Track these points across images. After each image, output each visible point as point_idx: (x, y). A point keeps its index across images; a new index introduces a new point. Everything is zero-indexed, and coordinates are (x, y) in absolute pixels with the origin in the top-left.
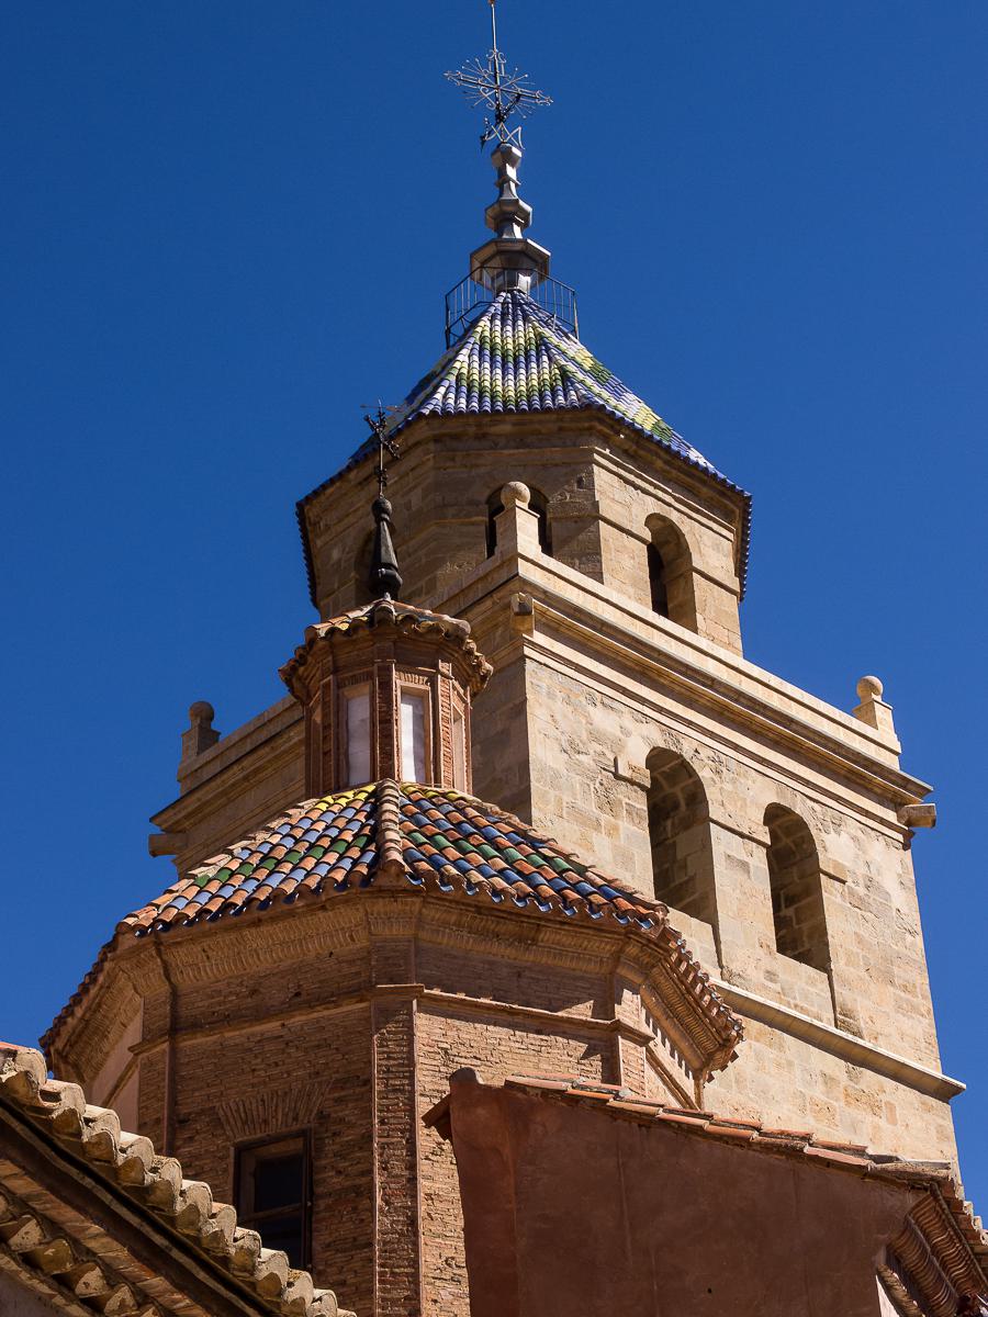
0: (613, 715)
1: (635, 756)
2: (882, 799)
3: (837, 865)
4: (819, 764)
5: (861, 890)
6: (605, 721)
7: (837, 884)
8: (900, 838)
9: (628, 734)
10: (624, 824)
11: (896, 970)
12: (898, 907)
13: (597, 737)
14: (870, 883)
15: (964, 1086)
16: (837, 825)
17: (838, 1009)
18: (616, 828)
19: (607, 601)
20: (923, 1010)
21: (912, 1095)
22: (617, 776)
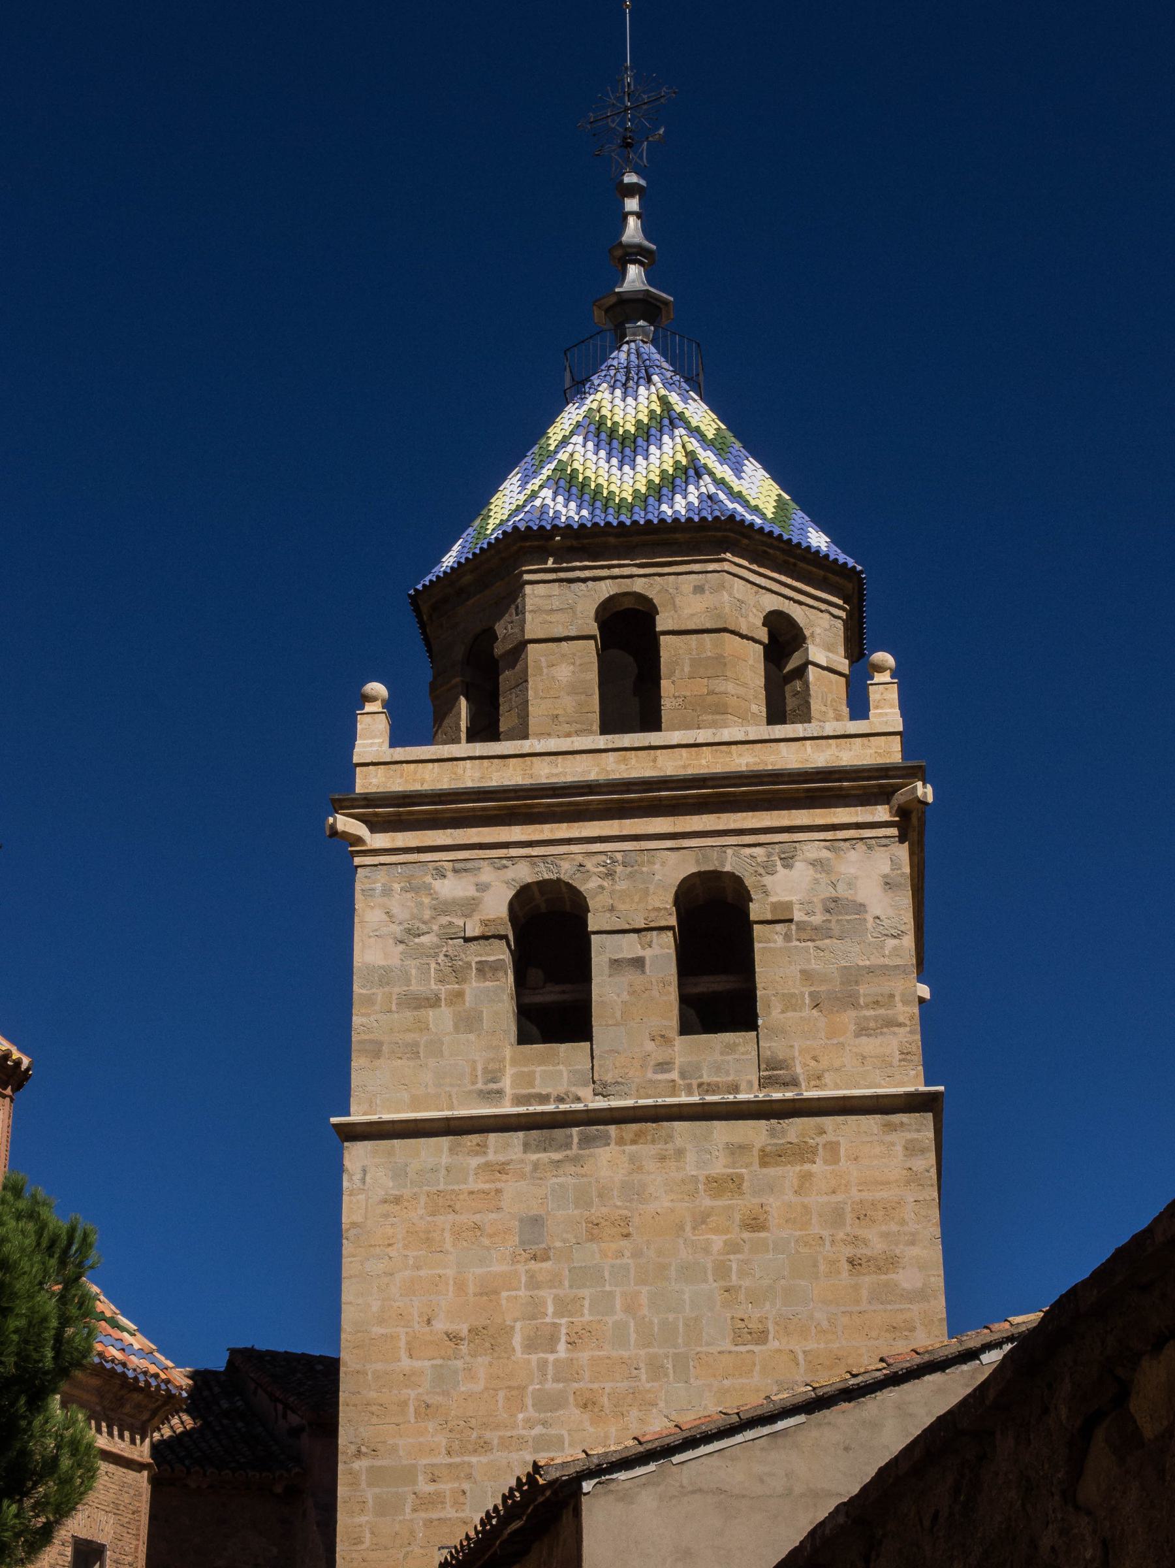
3: (775, 906)
5: (818, 919)
6: (451, 888)
8: (894, 831)
9: (482, 887)
10: (474, 986)
12: (878, 913)
13: (443, 908)
14: (834, 905)
15: (941, 1088)
16: (787, 861)
17: (763, 1066)
18: (460, 995)
20: (901, 1019)
21: (872, 1122)
22: (467, 940)
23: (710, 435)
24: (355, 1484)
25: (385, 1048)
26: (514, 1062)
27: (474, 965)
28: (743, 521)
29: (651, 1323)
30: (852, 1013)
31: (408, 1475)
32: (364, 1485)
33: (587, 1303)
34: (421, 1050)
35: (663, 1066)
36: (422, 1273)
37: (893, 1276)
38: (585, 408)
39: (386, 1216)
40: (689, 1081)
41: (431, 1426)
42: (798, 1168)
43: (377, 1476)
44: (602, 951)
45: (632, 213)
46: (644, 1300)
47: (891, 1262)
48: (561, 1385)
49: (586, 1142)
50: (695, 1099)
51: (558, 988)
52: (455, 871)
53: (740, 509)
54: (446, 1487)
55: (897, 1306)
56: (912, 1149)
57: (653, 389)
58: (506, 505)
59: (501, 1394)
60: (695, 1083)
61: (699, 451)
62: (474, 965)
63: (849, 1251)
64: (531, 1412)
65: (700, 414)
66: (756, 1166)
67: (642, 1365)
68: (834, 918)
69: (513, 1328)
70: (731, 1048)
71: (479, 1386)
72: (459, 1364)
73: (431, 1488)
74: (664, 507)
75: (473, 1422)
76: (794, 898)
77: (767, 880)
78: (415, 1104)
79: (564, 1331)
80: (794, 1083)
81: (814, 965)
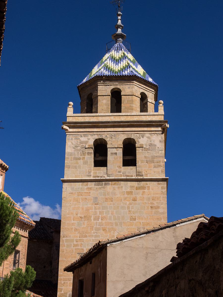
0: (86, 137)
1: (91, 142)
2: (157, 126)
4: (140, 126)
5: (148, 147)
6: (83, 139)
7: (141, 148)
8: (161, 132)
9: (89, 139)
10: (87, 156)
11: (155, 160)
13: (81, 142)
14: (151, 145)
15: (168, 178)
16: (143, 137)
17: (137, 173)
18: (84, 158)
19: (87, 116)
22: (85, 148)
23: (132, 60)
24: (63, 242)
25: (71, 167)
26: (93, 170)
27: (87, 153)
28: (137, 76)
29: (116, 216)
30: (153, 164)
31: (72, 241)
32: (65, 242)
33: (105, 212)
34: (77, 167)
35: (120, 172)
36: (76, 206)
37: (159, 210)
38: (110, 54)
39: (70, 196)
40: (124, 175)
41: (77, 232)
42: (142, 191)
43: (67, 241)
44: (110, 151)
45: (119, 19)
46: (115, 212)
47: (158, 207)
48: (100, 226)
49: (105, 184)
50: (125, 178)
51: (102, 157)
52: (84, 136)
53: (137, 74)
54: (79, 243)
55: (158, 215)
56: (162, 188)
57: (122, 51)
58: (95, 71)
59: (89, 228)
60: (125, 175)
61: (130, 63)
62: (87, 153)
63: (151, 205)
64: (94, 231)
65: (130, 56)
66: (135, 190)
67: (114, 224)
68: (151, 147)
69: (91, 216)
70: (132, 169)
71: (85, 226)
72: (82, 222)
73: (76, 243)
74: (123, 73)
75: (84, 232)
76: (144, 143)
77: (139, 140)
78: (76, 177)
79: (100, 217)
80: (142, 176)
81: (147, 155)
